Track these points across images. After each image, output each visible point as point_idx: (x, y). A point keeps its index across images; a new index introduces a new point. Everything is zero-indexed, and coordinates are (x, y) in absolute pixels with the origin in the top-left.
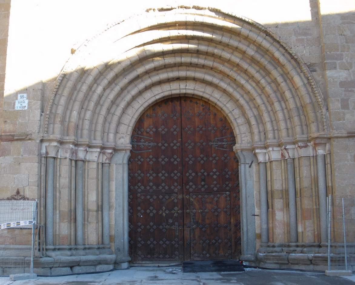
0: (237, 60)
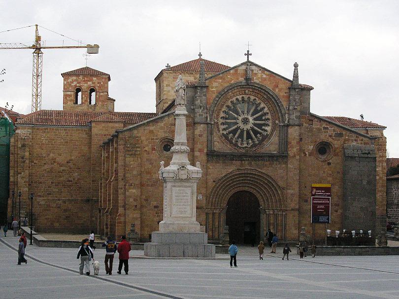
0: (262, 183)
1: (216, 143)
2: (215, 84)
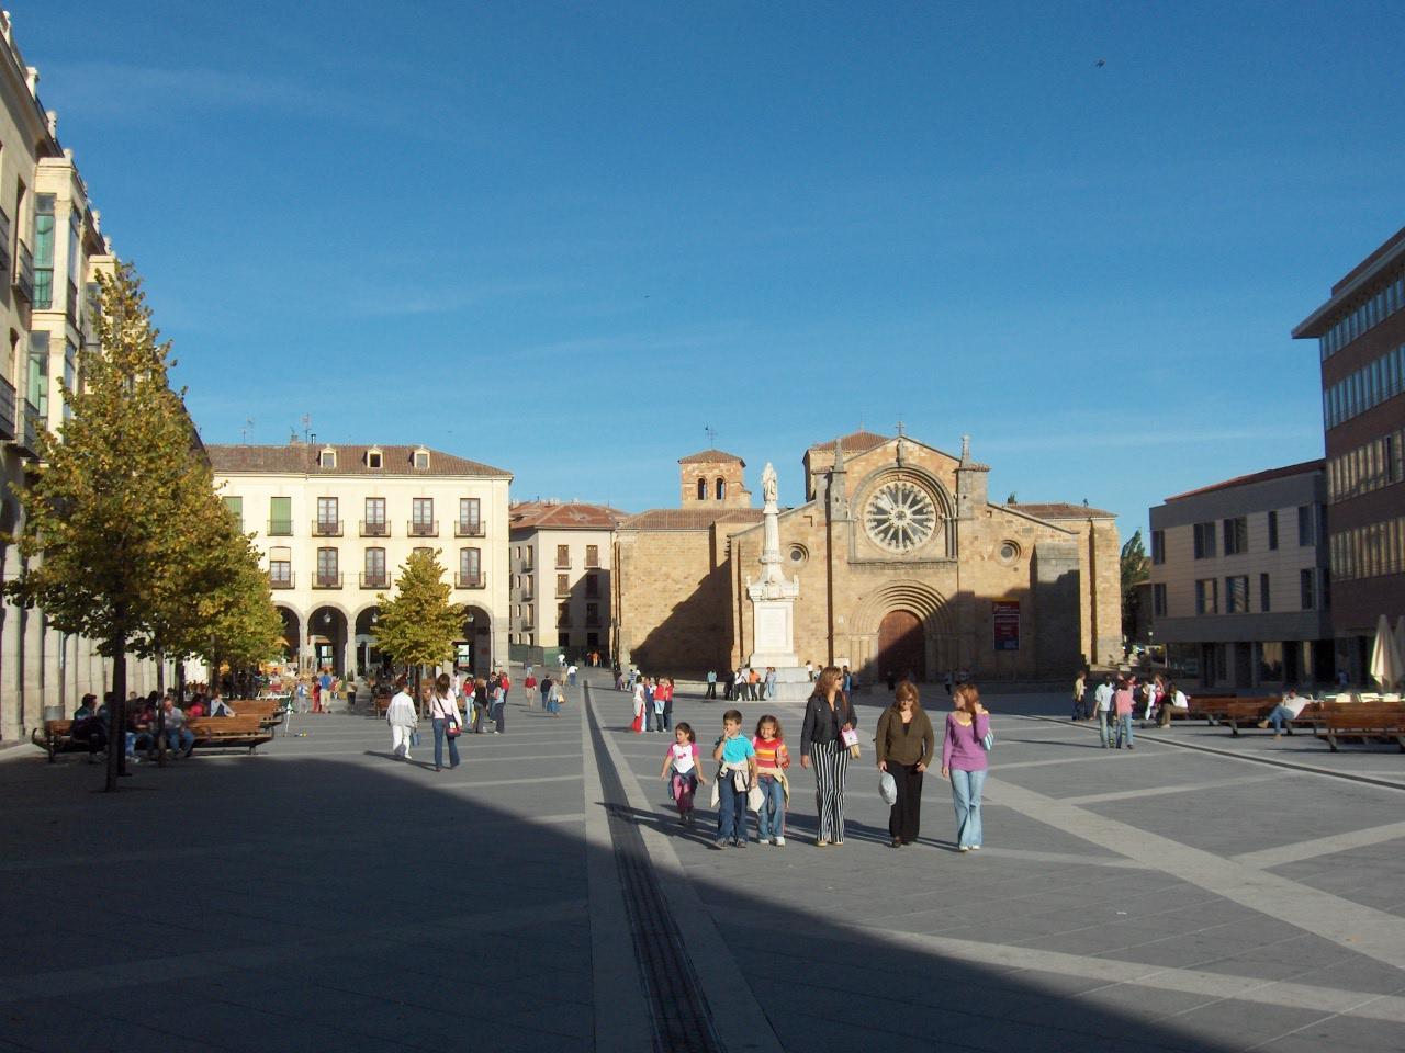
1: (861, 547)
2: (856, 468)
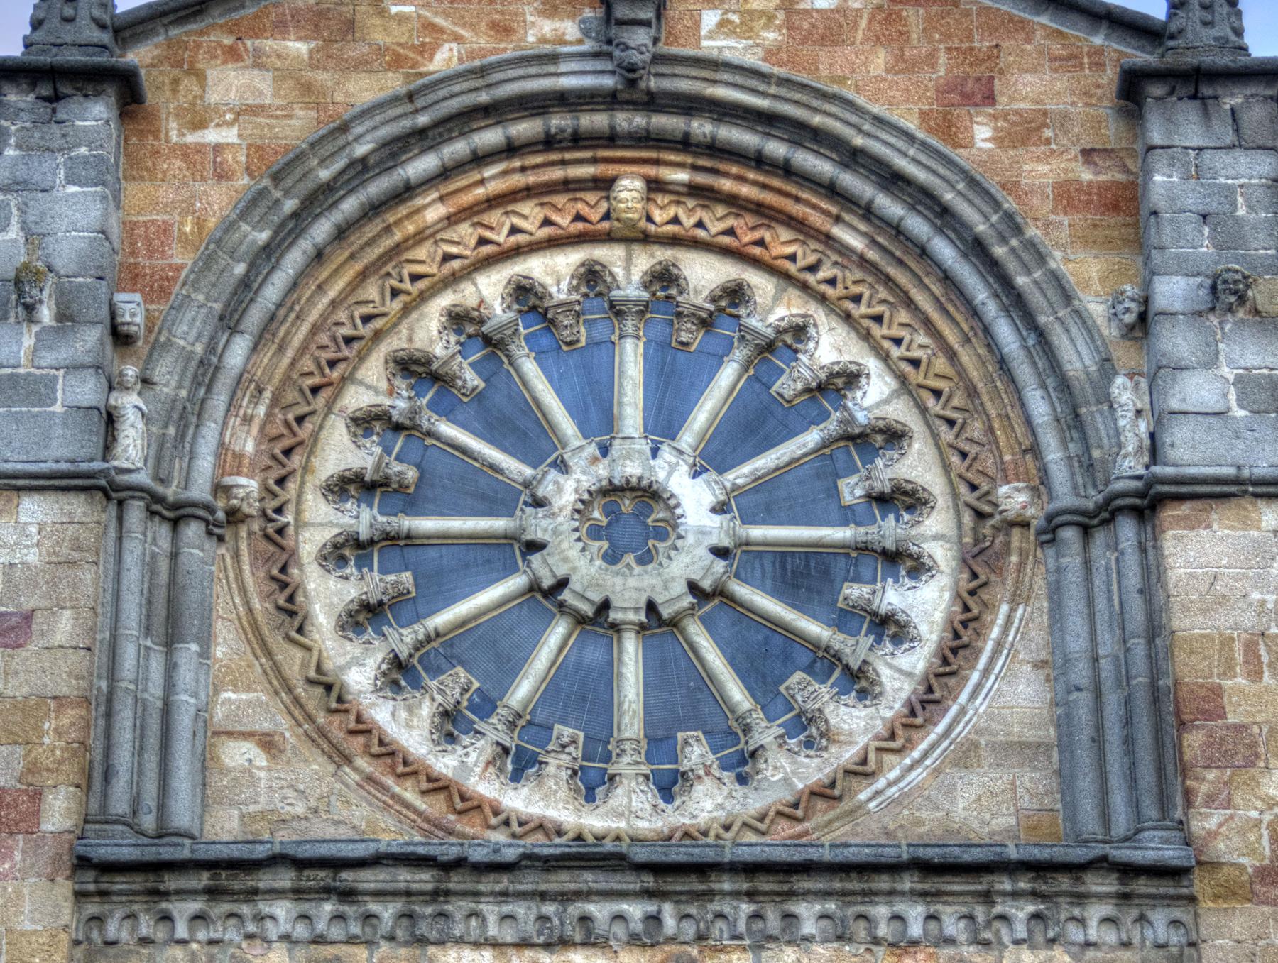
1: (237, 754)
2: (229, 84)
